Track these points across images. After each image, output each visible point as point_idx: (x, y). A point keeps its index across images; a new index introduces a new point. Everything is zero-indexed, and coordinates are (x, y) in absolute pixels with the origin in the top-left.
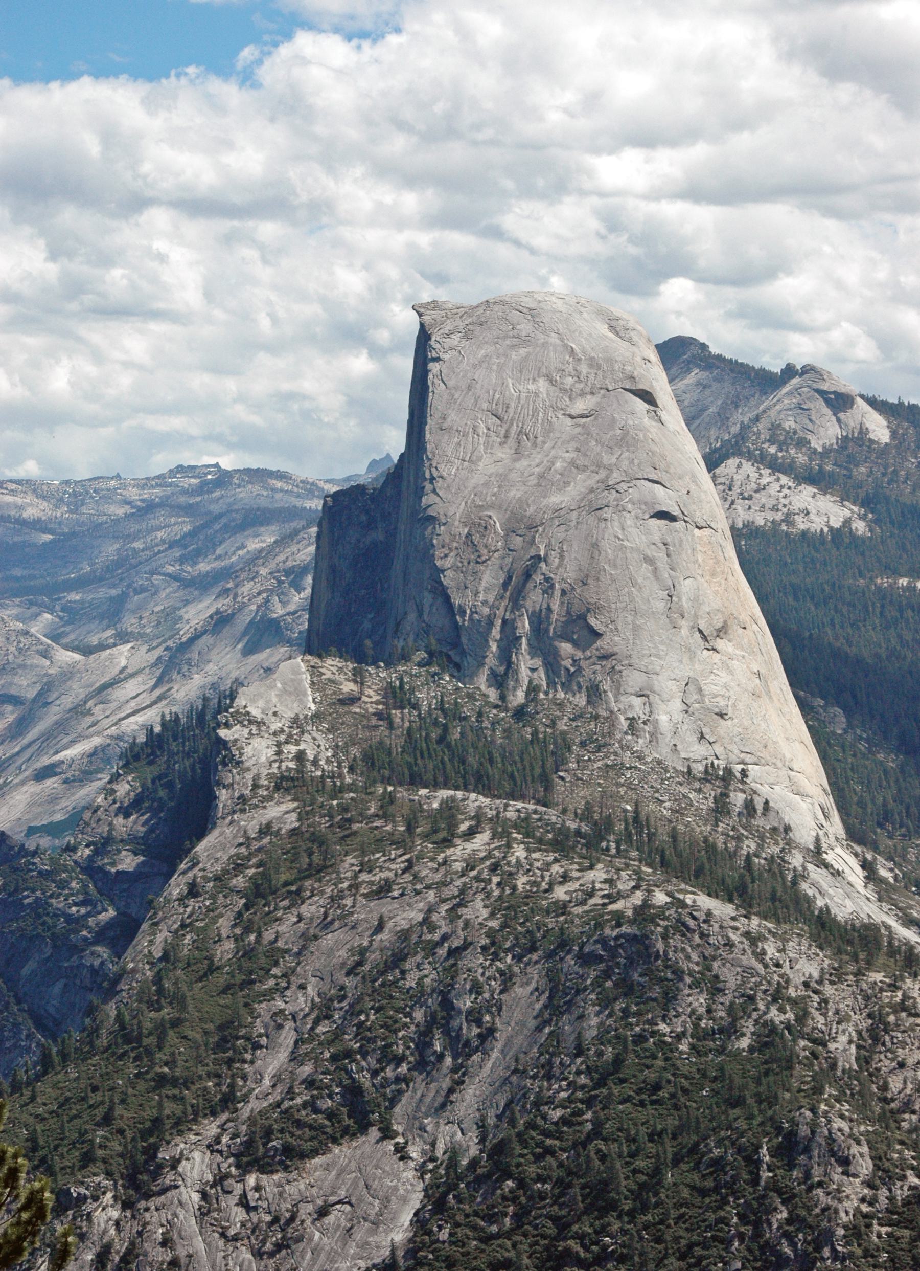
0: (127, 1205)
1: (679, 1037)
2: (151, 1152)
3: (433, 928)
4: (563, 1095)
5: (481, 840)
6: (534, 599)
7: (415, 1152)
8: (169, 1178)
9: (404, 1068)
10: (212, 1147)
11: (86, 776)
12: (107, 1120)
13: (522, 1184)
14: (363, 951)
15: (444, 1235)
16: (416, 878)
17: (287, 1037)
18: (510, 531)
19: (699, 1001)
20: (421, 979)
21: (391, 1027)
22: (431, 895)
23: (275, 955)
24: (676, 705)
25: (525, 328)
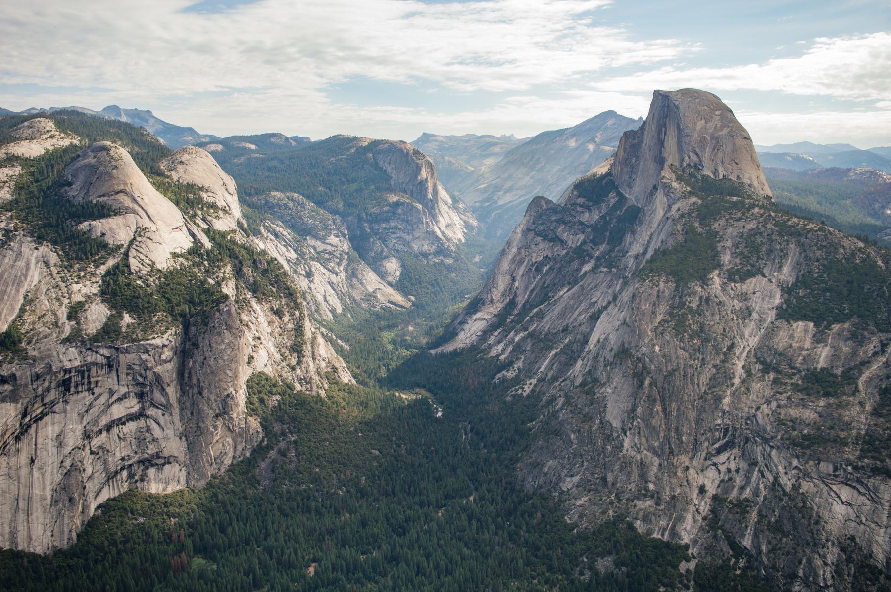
0: (702, 287)
1: (842, 259)
2: (705, 276)
3: (760, 229)
4: (817, 270)
5: (757, 210)
6: (720, 155)
7: (774, 281)
8: (711, 282)
9: (764, 261)
10: (719, 275)
11: (485, 192)
12: (692, 268)
13: (813, 290)
14: (742, 233)
15: (795, 301)
16: (747, 217)
17: (728, 252)
18: (711, 139)
19: (842, 251)
20: (762, 241)
21: (758, 252)
22: (755, 222)
23: (717, 233)
24: (756, 182)
25: (697, 95)
